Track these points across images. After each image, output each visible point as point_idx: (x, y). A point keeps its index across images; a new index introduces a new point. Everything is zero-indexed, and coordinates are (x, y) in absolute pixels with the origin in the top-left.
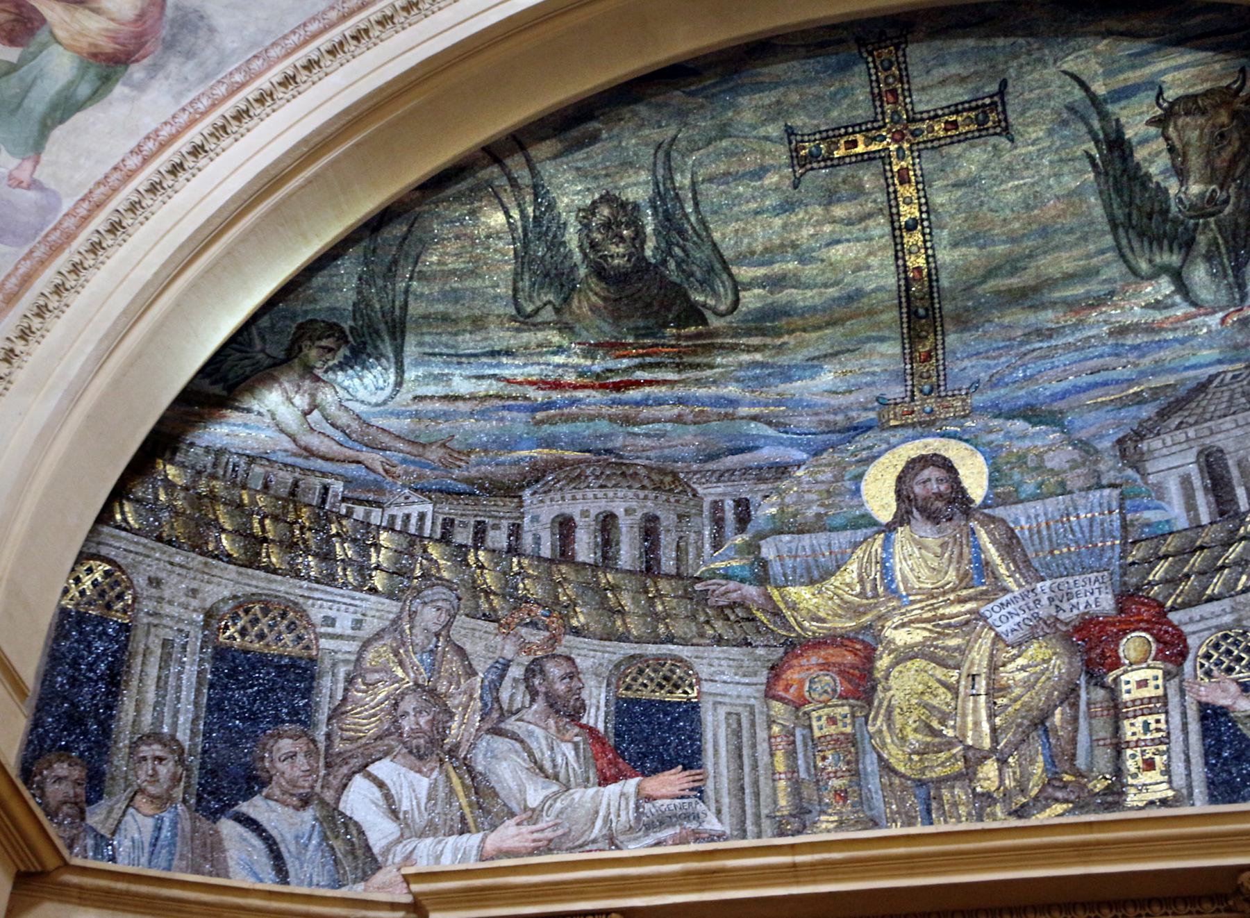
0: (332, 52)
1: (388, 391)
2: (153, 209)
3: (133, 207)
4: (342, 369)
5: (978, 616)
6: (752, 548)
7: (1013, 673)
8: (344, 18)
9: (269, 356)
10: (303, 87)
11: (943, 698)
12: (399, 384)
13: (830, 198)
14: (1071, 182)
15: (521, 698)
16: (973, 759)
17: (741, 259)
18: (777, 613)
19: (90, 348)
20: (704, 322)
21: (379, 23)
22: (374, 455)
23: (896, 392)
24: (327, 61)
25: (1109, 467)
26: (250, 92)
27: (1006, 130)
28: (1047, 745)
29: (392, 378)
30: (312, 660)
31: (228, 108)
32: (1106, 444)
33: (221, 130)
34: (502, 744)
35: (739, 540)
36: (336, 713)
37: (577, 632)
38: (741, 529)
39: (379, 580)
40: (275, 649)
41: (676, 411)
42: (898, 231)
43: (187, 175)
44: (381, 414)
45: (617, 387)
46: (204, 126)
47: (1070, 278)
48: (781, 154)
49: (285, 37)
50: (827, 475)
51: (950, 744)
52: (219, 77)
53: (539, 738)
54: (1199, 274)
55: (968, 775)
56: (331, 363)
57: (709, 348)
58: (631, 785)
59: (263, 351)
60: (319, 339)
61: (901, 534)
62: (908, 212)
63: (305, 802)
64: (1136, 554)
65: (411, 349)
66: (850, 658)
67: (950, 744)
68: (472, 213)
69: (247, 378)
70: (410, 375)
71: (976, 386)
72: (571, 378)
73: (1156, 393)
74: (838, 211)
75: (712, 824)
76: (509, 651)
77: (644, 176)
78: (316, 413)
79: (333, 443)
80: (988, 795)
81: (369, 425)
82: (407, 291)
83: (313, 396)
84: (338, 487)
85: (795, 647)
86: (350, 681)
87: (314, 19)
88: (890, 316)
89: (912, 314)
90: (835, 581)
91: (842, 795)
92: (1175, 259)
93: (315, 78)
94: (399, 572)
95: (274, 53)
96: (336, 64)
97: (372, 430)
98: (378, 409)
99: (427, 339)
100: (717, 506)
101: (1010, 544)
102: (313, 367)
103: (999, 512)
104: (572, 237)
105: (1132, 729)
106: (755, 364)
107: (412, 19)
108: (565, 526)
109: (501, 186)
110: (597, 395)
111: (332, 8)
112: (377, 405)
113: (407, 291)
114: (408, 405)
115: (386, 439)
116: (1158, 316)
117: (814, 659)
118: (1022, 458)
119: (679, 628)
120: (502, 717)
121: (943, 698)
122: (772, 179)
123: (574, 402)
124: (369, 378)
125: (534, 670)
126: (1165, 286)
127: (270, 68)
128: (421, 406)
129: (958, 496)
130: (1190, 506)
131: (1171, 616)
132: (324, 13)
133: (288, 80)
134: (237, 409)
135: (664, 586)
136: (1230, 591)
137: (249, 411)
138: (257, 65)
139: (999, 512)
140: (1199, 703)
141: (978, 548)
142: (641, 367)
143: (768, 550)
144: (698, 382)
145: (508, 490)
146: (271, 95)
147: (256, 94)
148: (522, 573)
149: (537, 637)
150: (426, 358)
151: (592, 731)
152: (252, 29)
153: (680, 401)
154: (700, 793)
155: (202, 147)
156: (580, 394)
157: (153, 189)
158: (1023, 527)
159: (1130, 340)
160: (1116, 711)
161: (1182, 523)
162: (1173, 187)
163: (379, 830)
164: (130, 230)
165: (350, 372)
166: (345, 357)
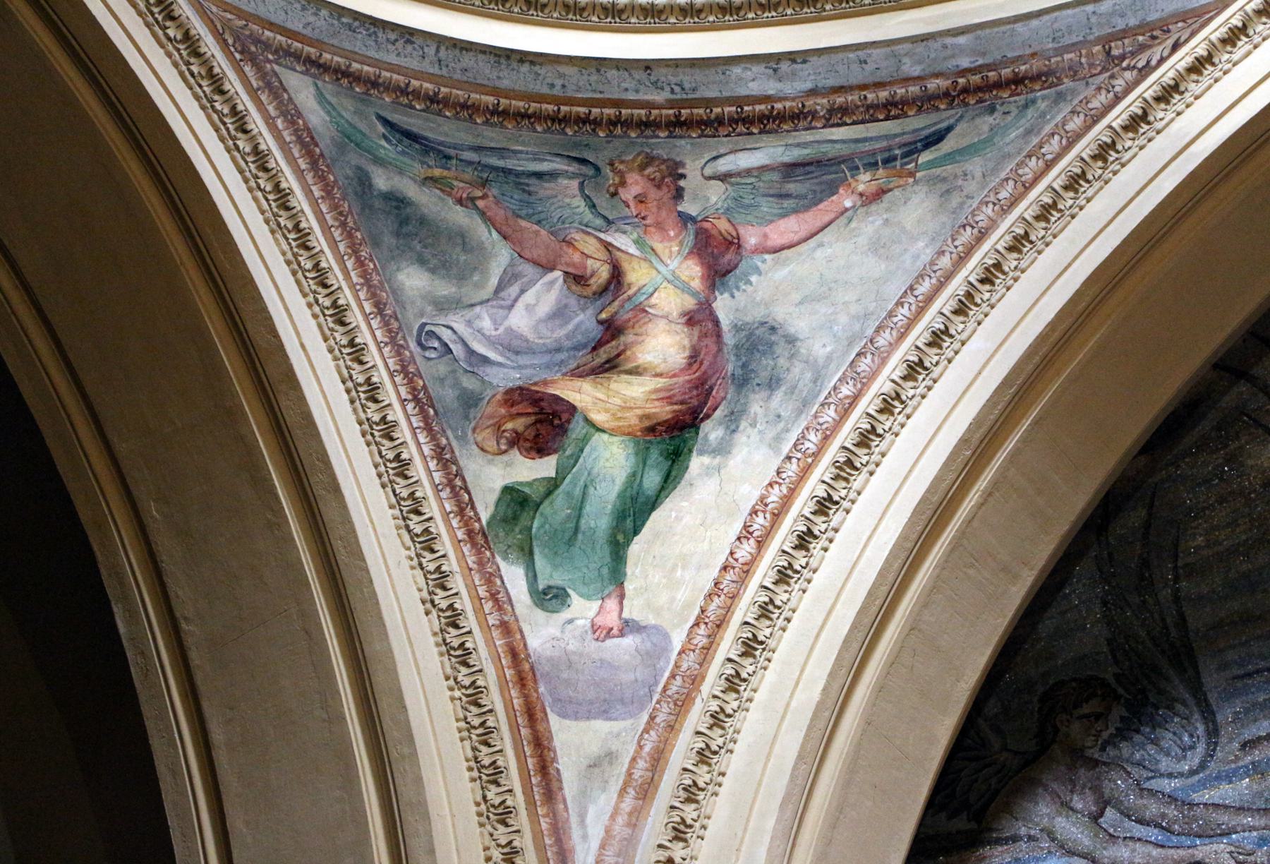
0: (961, 311)
1: (1201, 748)
2: (791, 605)
3: (765, 611)
4: (1125, 739)
8: (962, 260)
9: (1016, 753)
10: (936, 372)
19: (771, 823)
21: (1011, 249)
22: (1215, 847)
24: (957, 325)
26: (868, 403)
29: (1201, 729)
31: (846, 435)
33: (846, 468)
43: (823, 542)
44: (1203, 785)
46: (823, 469)
49: (891, 314)
52: (821, 398)
56: (1105, 735)
59: (1005, 748)
60: (1075, 707)
65: (1212, 680)
68: (1231, 459)
69: (997, 792)
70: (1225, 715)
78: (1110, 813)
79: (1150, 848)
81: (1192, 805)
82: (1176, 599)
83: (1097, 790)
87: (921, 276)
93: (949, 353)
95: (882, 341)
96: (971, 325)
97: (1199, 811)
98: (1196, 778)
99: (1231, 655)
102: (1082, 750)
107: (1054, 228)
109: (1260, 408)
111: (941, 253)
112: (1193, 772)
113: (1176, 599)
114: (1237, 758)
115: (1224, 818)
124: (1167, 739)
127: (884, 361)
128: (1257, 755)
132: (932, 263)
133: (914, 370)
134: (998, 842)
137: (1015, 839)
138: (865, 364)
146: (898, 396)
147: (878, 403)
150: (1239, 684)
152: (843, 319)
155: (830, 498)
157: (783, 577)
164: (771, 643)
165: (1138, 738)
166: (1122, 719)
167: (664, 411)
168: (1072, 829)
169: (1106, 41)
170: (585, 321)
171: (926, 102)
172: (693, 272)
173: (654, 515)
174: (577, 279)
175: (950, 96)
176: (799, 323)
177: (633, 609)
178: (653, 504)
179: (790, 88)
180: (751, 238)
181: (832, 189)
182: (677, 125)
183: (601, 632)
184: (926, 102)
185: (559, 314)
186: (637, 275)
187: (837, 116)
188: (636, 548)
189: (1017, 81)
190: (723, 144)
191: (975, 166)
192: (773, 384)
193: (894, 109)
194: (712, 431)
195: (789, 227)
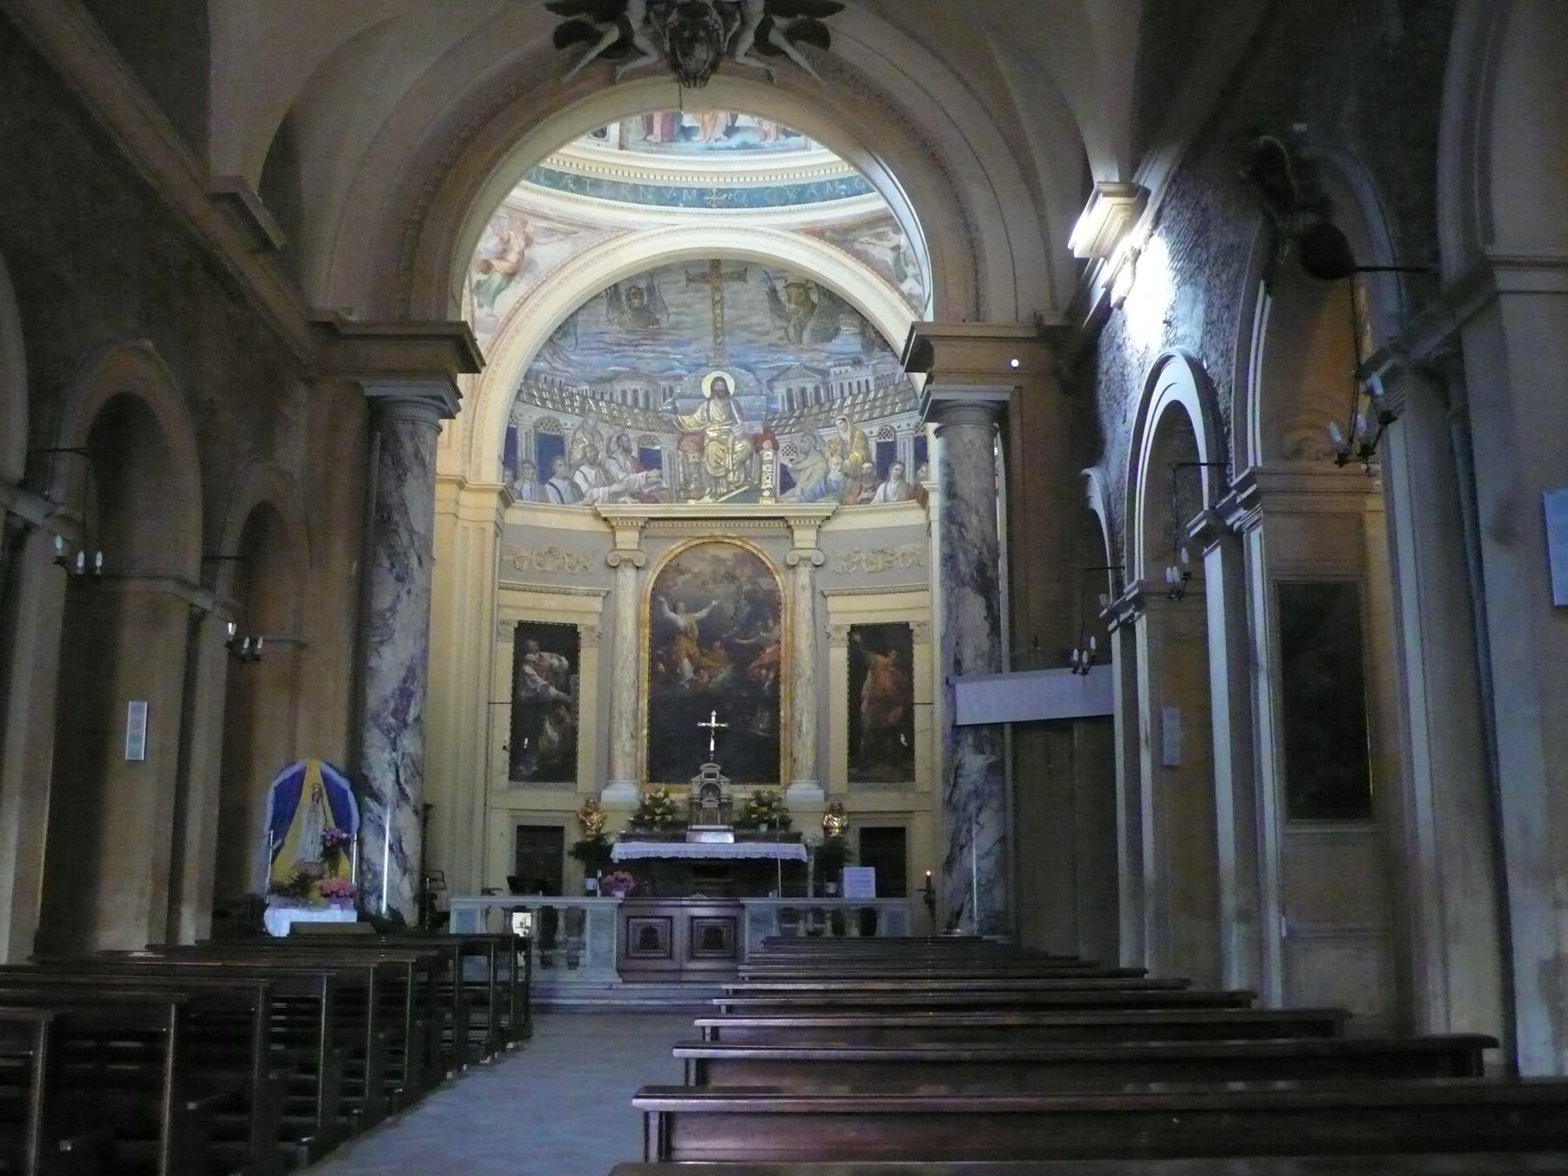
5: (730, 430)
6: (673, 403)
7: (738, 447)
11: (720, 454)
12: (577, 344)
13: (697, 291)
14: (761, 297)
15: (616, 447)
16: (728, 471)
17: (672, 305)
18: (679, 424)
20: (659, 324)
23: (711, 354)
25: (765, 390)
27: (745, 281)
28: (745, 469)
30: (562, 437)
32: (764, 381)
34: (612, 461)
35: (670, 400)
36: (570, 452)
37: (629, 427)
38: (671, 396)
39: (577, 410)
40: (553, 433)
41: (652, 355)
42: (715, 303)
45: (636, 346)
47: (758, 325)
48: (683, 278)
50: (692, 380)
51: (720, 466)
53: (621, 459)
54: (791, 331)
55: (726, 476)
57: (660, 334)
58: (644, 473)
61: (712, 402)
62: (717, 298)
63: (565, 478)
64: (770, 417)
66: (697, 438)
67: (720, 466)
71: (732, 356)
72: (623, 342)
73: (778, 367)
74: (699, 295)
75: (664, 485)
76: (611, 432)
77: (645, 281)
80: (730, 483)
84: (563, 380)
85: (685, 435)
86: (572, 443)
88: (710, 328)
89: (716, 328)
90: (695, 416)
91: (696, 479)
92: (785, 324)
94: (582, 408)
100: (665, 390)
101: (739, 409)
103: (737, 398)
104: (624, 298)
105: (764, 468)
106: (674, 340)
108: (624, 393)
110: (631, 349)
116: (780, 342)
117: (690, 438)
118: (743, 381)
119: (655, 427)
120: (613, 452)
121: (720, 454)
122: (680, 284)
123: (624, 351)
125: (619, 438)
126: (782, 333)
129: (727, 392)
130: (783, 405)
131: (777, 437)
135: (651, 414)
136: (790, 433)
139: (737, 398)
140: (781, 464)
141: (731, 410)
142: (644, 339)
143: (678, 405)
144: (661, 346)
145: (609, 380)
148: (614, 409)
149: (618, 428)
151: (633, 457)
153: (653, 352)
154: (661, 476)
156: (627, 348)
158: (742, 404)
159: (773, 348)
160: (762, 463)
161: (781, 410)
162: (787, 304)
163: (584, 487)
167: (510, 271)
168: (548, 357)
169: (613, 227)
170: (500, 247)
171: (577, 225)
172: (523, 243)
173: (503, 293)
174: (501, 239)
175: (581, 226)
176: (539, 261)
177: (495, 312)
178: (503, 290)
179: (552, 214)
180: (536, 240)
181: (553, 236)
182: (529, 214)
183: (488, 315)
184: (577, 225)
185: (497, 245)
186: (512, 241)
187: (560, 222)
188: (498, 299)
189: (595, 228)
190: (535, 219)
191: (581, 241)
192: (531, 272)
193: (571, 224)
194: (517, 278)
195: (543, 240)
